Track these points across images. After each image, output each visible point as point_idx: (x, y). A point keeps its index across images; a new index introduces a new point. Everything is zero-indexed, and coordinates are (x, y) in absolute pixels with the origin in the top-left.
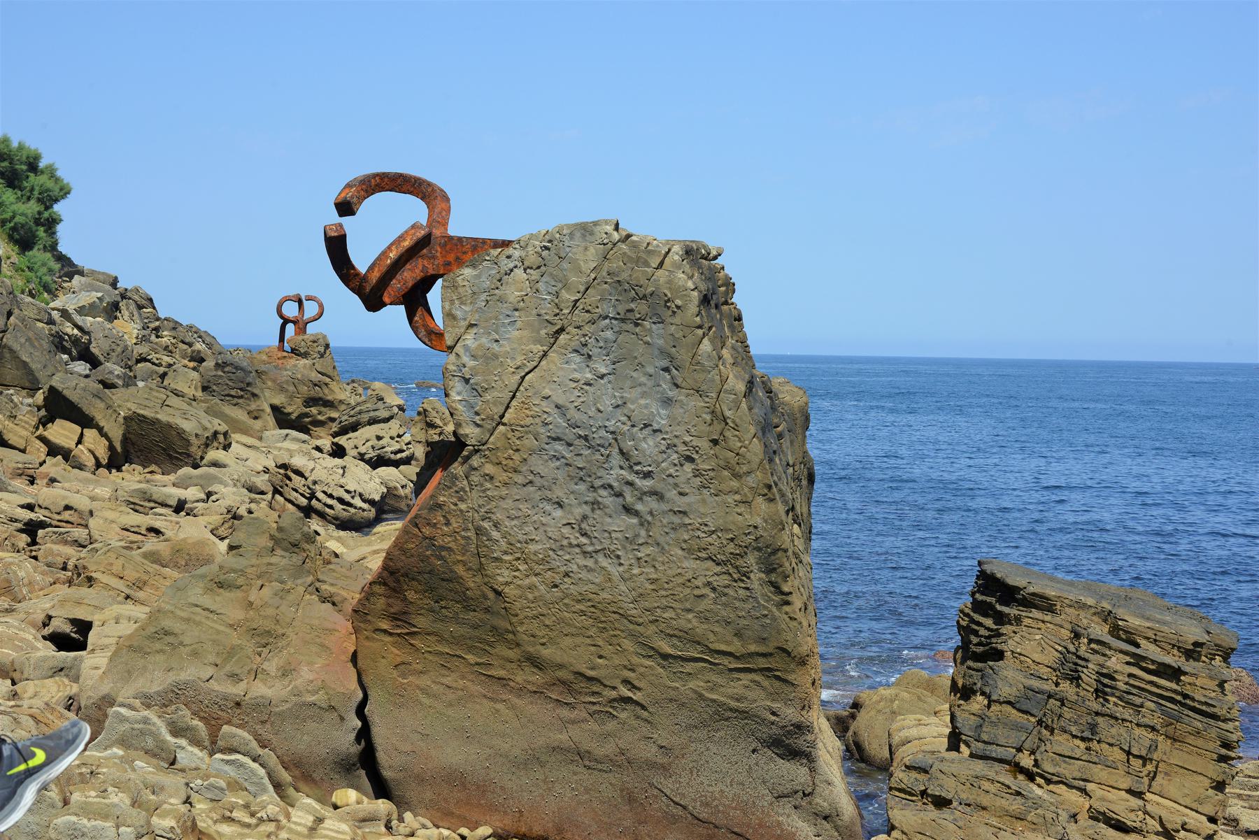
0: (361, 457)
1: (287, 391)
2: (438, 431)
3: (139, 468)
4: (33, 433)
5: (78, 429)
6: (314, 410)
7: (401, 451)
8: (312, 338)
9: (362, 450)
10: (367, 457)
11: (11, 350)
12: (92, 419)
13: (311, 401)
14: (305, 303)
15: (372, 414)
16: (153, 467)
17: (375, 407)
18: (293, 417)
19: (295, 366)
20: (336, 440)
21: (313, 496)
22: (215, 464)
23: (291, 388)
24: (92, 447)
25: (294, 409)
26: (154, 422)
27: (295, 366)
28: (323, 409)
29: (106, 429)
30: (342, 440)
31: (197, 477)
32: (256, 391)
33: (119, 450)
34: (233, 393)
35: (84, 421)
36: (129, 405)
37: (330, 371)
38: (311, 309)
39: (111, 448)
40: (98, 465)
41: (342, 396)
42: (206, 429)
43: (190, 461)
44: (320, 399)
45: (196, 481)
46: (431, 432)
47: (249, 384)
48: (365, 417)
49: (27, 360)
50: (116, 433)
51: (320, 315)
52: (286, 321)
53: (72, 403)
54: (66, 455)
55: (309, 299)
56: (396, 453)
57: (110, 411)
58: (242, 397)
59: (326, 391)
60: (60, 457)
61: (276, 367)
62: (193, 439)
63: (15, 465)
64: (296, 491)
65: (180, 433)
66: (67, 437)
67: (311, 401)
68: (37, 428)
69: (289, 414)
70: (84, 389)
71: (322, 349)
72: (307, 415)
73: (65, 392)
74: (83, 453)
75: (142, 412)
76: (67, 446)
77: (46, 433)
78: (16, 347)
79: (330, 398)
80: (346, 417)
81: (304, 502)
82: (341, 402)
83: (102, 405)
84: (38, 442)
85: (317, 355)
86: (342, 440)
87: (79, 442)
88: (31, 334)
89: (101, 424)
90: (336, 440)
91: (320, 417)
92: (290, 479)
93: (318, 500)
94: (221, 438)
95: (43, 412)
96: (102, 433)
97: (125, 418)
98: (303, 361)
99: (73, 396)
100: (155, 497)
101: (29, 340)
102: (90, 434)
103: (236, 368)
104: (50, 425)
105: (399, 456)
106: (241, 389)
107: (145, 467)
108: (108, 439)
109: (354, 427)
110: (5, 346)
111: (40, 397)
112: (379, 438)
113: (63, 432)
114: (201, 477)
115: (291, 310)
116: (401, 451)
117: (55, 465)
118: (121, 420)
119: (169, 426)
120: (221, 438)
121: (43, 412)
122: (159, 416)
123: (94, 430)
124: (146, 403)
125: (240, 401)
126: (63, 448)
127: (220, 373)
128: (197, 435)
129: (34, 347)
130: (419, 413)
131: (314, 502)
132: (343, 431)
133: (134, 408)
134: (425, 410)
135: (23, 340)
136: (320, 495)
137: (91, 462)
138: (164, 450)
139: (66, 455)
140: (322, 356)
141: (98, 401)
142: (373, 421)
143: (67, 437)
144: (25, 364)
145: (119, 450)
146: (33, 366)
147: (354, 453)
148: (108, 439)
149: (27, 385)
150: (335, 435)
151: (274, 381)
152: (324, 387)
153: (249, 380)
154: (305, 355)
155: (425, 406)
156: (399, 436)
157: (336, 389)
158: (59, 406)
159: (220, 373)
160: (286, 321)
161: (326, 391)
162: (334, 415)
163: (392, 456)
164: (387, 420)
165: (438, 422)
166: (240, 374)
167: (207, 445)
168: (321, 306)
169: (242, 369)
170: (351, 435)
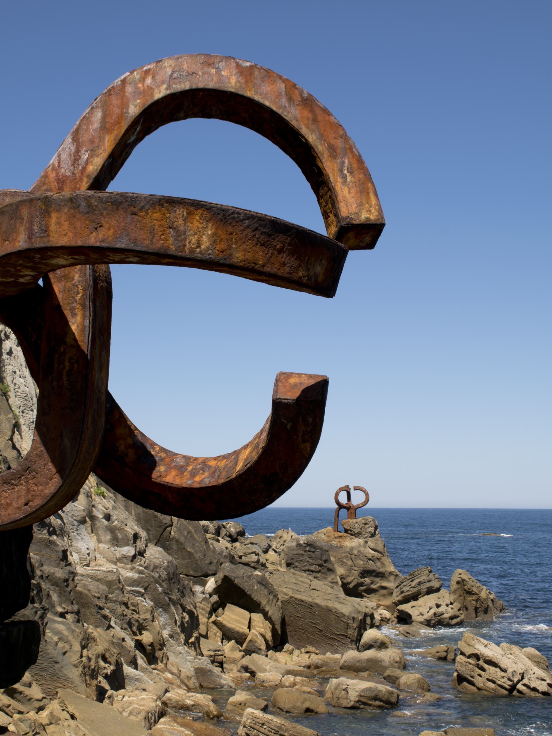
2: (475, 597)
5: (247, 613)
6: (367, 580)
13: (365, 573)
14: (352, 492)
15: (428, 585)
16: (310, 648)
18: (351, 586)
24: (262, 631)
25: (353, 579)
32: (330, 566)
34: (312, 568)
35: (251, 606)
36: (285, 590)
38: (357, 498)
39: (274, 630)
40: (268, 648)
42: (359, 612)
44: (374, 571)
46: (470, 598)
48: (424, 588)
50: (276, 616)
51: (367, 502)
53: (239, 588)
57: (271, 597)
58: (319, 572)
60: (233, 642)
66: (239, 622)
69: (349, 583)
72: (362, 584)
76: (241, 630)
79: (382, 570)
80: (408, 588)
82: (391, 573)
84: (215, 627)
91: (373, 586)
92: (483, 669)
95: (215, 598)
102: (257, 617)
104: (220, 610)
106: (320, 565)
109: (415, 597)
112: (438, 606)
113: (234, 617)
119: (329, 610)
121: (215, 598)
122: (318, 601)
125: (318, 575)
128: (354, 618)
132: (406, 600)
134: (463, 580)
137: (263, 647)
142: (430, 591)
143: (239, 622)
145: (280, 632)
149: (191, 572)
154: (357, 535)
156: (451, 604)
158: (231, 593)
159: (301, 552)
160: (341, 506)
161: (379, 564)
162: (385, 584)
164: (438, 590)
165: (475, 590)
168: (367, 495)
170: (413, 603)
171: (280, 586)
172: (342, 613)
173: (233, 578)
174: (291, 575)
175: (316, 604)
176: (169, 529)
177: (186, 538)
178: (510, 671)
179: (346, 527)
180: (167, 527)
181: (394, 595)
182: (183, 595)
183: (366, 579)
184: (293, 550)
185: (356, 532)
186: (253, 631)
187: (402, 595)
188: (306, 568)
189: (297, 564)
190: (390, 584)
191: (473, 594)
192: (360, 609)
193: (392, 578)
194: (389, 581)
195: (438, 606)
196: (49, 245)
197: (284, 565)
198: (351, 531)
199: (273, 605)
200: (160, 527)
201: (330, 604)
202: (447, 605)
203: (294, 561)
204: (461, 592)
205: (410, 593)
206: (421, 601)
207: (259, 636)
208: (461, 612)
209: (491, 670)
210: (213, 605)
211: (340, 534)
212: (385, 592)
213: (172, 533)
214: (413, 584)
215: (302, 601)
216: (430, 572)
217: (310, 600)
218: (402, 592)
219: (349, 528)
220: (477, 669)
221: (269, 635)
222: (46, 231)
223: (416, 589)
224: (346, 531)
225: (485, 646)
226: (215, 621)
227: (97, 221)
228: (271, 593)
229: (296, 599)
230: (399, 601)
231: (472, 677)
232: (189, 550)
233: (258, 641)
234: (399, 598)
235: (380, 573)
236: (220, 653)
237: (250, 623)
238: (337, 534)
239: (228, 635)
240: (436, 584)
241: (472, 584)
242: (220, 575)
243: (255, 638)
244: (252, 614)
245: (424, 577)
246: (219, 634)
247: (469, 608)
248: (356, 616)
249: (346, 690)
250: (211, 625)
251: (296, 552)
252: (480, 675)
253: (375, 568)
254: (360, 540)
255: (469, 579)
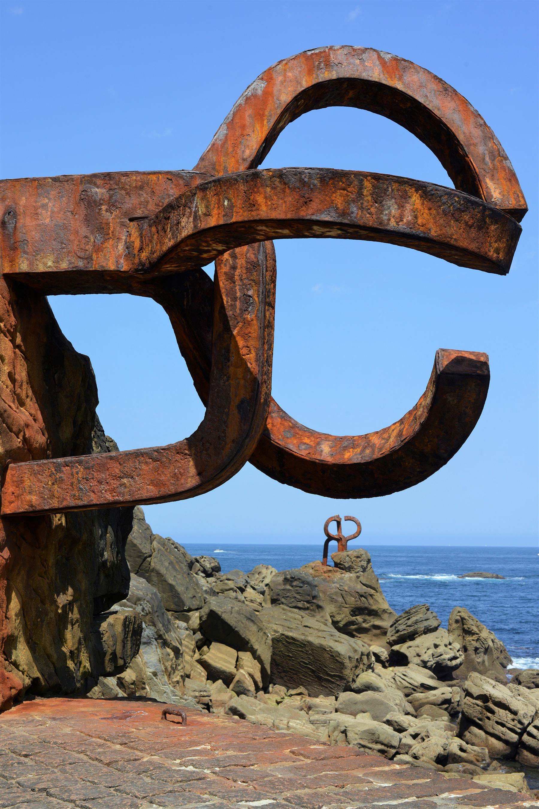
0: (424, 664)
1: (336, 601)
2: (475, 637)
3: (283, 689)
4: (192, 657)
5: (233, 652)
6: (359, 619)
7: (455, 658)
8: (355, 554)
9: (425, 657)
10: (429, 664)
11: (159, 574)
12: (248, 642)
13: (358, 611)
14: (343, 522)
15: (426, 624)
16: (301, 689)
17: (425, 617)
19: (342, 579)
20: (396, 648)
21: (524, 730)
22: (368, 687)
23: (340, 599)
24: (251, 671)
25: (344, 617)
26: (305, 645)
27: (342, 579)
28: (367, 617)
29: (259, 652)
30: (403, 648)
31: (362, 702)
32: (320, 603)
33: (269, 672)
34: (300, 605)
35: (239, 643)
36: (275, 627)
37: (373, 583)
38: (348, 529)
39: (263, 671)
40: (257, 689)
41: (385, 606)
42: (355, 651)
43: (343, 684)
44: (366, 608)
45: (361, 707)
46: (469, 638)
47: (314, 597)
48: (421, 627)
49: (173, 583)
50: (266, 655)
51: (359, 533)
52: (330, 538)
54: (228, 679)
55: (348, 519)
56: (451, 660)
57: (261, 634)
58: (307, 609)
59: (371, 601)
60: (220, 681)
61: (324, 580)
62: (347, 662)
63: (192, 694)
64: (503, 725)
65: (335, 657)
67: (358, 611)
68: (194, 652)
70: (239, 613)
71: (364, 563)
72: (352, 623)
73: (225, 617)
74: (242, 675)
75: (290, 634)
76: (228, 670)
77: (205, 657)
78: (163, 571)
79: (374, 607)
80: (404, 627)
81: (514, 737)
82: (384, 611)
83: (254, 628)
84: (199, 666)
85: (360, 569)
86: (403, 648)
87: (237, 667)
88: (172, 558)
89: (256, 647)
90: (396, 648)
91: (365, 625)
92: (493, 712)
93: (530, 735)
94: (365, 658)
95: (199, 636)
96: (254, 653)
97: (273, 640)
98: (347, 575)
99: (231, 619)
100: (382, 738)
101: (171, 563)
102: (246, 657)
103: (303, 582)
104: (205, 648)
105: (454, 663)
106: (308, 602)
107: (288, 688)
108: (261, 661)
109: (412, 637)
110: (153, 570)
111: (195, 618)
112: (436, 646)
113: (220, 655)
114: (367, 702)
115: (333, 529)
116: (455, 658)
117: (220, 691)
118: (270, 642)
119: (322, 648)
120: (365, 658)
121: (199, 636)
122: (310, 639)
123: (249, 654)
124: (287, 624)
126: (223, 672)
127: (288, 587)
128: (350, 657)
129: (176, 570)
130: (457, 621)
131: (525, 737)
132: (402, 640)
133: (281, 630)
134: (463, 619)
135: (167, 564)
136: (531, 729)
137: (252, 688)
138: (313, 671)
139: (228, 679)
140: (364, 570)
141: (251, 624)
142: (429, 630)
144: (172, 587)
145: (269, 672)
146: (180, 589)
147: (417, 660)
148: (261, 661)
149: (173, 607)
150: (391, 644)
151: (324, 593)
152: (369, 598)
153: (314, 593)
154: (349, 569)
155: (463, 614)
156: (450, 644)
157: (380, 601)
158: (215, 630)
160: (330, 538)
161: (371, 601)
162: (377, 622)
163: (449, 663)
164: (435, 629)
165: (475, 629)
166: (306, 587)
167: (356, 667)
168: (359, 525)
169: (308, 583)
170: (410, 643)
171: (269, 622)
172: (337, 652)
173: (220, 613)
174: (281, 610)
175: (308, 642)
176: (149, 559)
177: (167, 569)
178: (521, 713)
179: (336, 561)
180: (146, 557)
181: (389, 634)
182: (168, 631)
183: (358, 617)
184: (280, 584)
185: (347, 565)
186: (241, 671)
187: (397, 635)
188: (294, 605)
189: (283, 600)
190: (385, 623)
191: (473, 634)
192: (357, 648)
193: (385, 616)
194: (382, 619)
195: (436, 646)
196: (257, 218)
197: (269, 602)
198: (342, 565)
199: (263, 642)
200: (139, 557)
201: (324, 642)
202: (446, 646)
203: (280, 597)
204: (460, 632)
205: (406, 632)
206: (418, 641)
207: (247, 676)
208: (460, 653)
209: (501, 713)
210: (197, 642)
211: (330, 568)
212: (378, 631)
213: (152, 564)
214: (409, 622)
215: (293, 639)
216: (428, 610)
217: (303, 637)
218: (398, 631)
219: (339, 561)
220: (485, 711)
221: (258, 677)
222: (253, 206)
223: (412, 629)
224: (337, 565)
225: (493, 687)
226: (200, 659)
227: (307, 195)
228: (260, 629)
229: (287, 637)
230: (393, 641)
231: (480, 720)
232: (171, 581)
233: (246, 681)
234: (394, 638)
235: (373, 610)
236: (205, 694)
237: (237, 661)
238: (326, 568)
239: (213, 674)
240: (433, 623)
241: (472, 623)
242: (205, 611)
243: (242, 678)
244: (239, 652)
245: (421, 615)
246: (204, 673)
247: (469, 648)
248: (352, 655)
249: (344, 732)
250: (196, 664)
251: (283, 587)
252: (489, 718)
253: (367, 605)
254: (351, 575)
255: (469, 617)
